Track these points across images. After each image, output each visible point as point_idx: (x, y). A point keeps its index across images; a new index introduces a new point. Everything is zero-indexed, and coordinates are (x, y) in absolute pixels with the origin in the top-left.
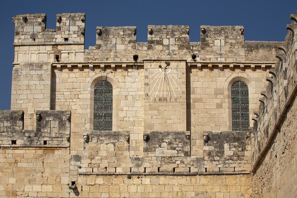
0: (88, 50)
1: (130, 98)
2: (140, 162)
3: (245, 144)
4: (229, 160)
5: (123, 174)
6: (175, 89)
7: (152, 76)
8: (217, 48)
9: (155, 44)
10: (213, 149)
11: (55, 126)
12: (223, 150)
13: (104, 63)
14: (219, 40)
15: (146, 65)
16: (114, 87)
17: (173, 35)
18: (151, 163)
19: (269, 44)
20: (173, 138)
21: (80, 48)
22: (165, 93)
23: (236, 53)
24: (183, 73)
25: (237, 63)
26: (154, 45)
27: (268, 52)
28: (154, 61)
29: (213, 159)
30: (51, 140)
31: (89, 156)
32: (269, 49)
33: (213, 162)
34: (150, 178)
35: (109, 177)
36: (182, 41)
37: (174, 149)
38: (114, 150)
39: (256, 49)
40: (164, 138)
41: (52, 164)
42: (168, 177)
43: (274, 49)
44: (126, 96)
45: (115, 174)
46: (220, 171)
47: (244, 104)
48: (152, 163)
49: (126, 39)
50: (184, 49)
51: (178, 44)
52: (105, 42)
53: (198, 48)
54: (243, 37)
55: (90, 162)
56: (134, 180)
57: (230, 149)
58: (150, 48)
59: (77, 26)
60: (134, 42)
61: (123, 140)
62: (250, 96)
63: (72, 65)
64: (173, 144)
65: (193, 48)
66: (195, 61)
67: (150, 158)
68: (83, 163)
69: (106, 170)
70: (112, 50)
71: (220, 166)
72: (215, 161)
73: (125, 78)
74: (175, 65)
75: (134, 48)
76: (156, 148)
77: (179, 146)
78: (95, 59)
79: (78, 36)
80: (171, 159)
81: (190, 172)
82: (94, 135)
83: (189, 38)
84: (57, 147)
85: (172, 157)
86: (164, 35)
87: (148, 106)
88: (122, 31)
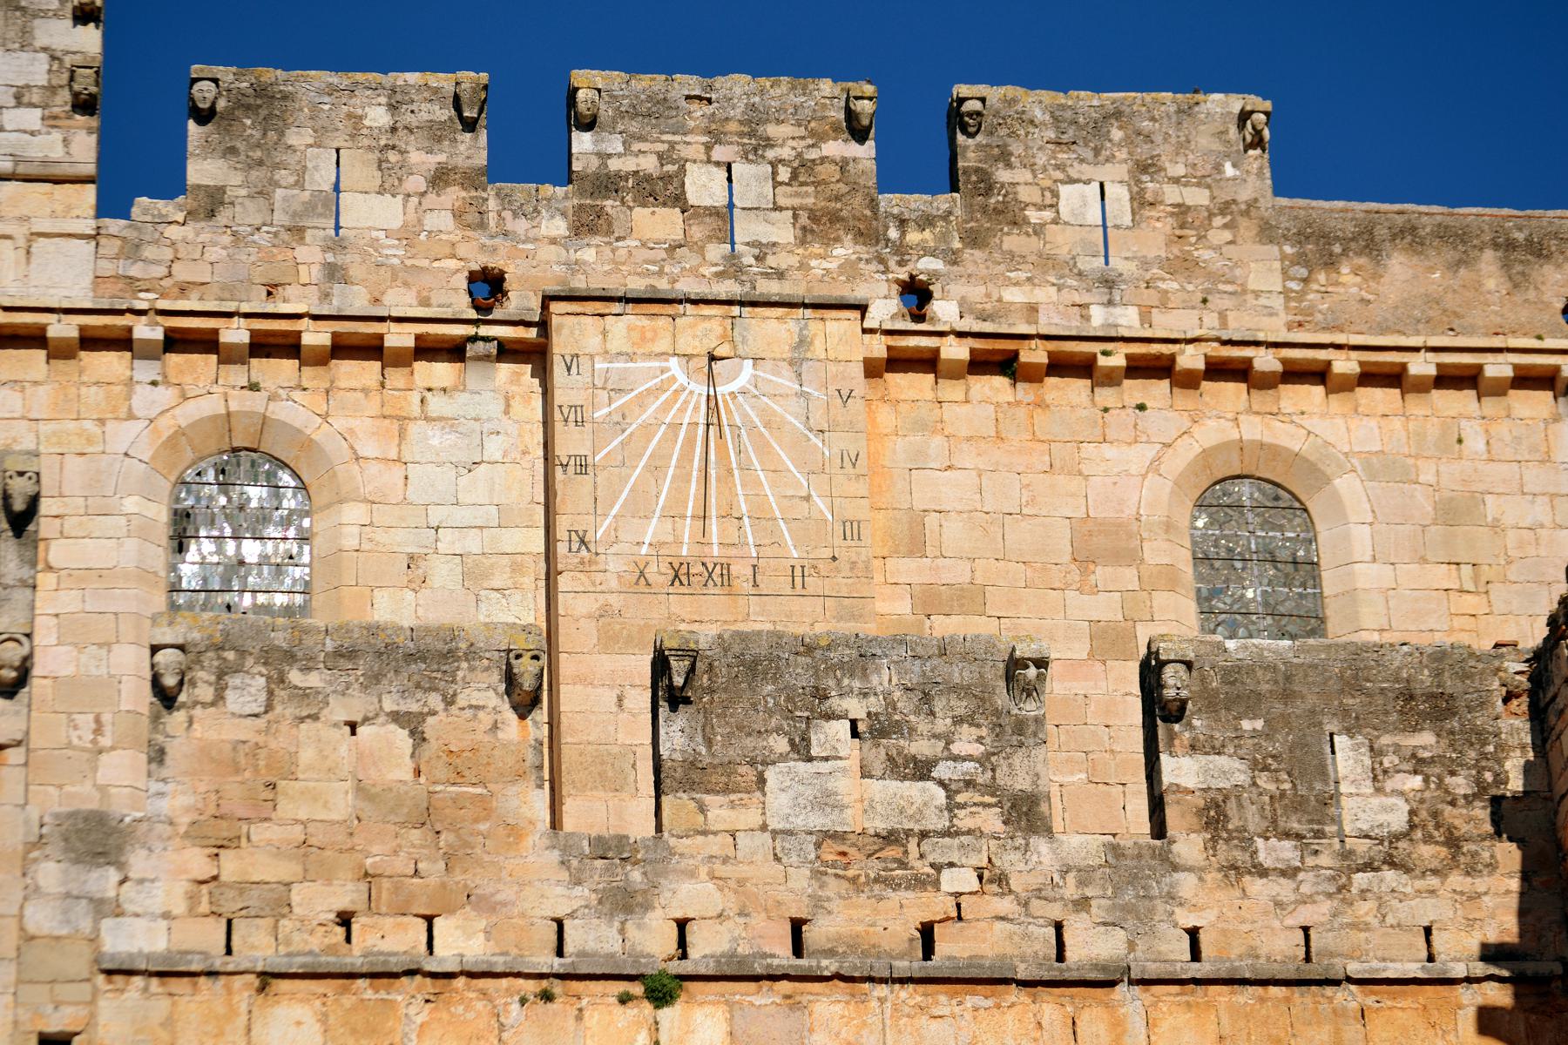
0: (123, 222)
2: (636, 875)
3: (1500, 747)
5: (499, 969)
6: (785, 502)
7: (613, 406)
9: (629, 198)
10: (1242, 778)
12: (1318, 786)
13: (247, 316)
14: (1087, 182)
15: (565, 331)
17: (757, 147)
18: (732, 884)
19: (1449, 221)
21: (69, 208)
23: (1215, 277)
24: (845, 393)
26: (623, 202)
29: (1241, 857)
31: (195, 817)
32: (1457, 256)
33: (1247, 878)
34: (727, 1002)
35: (369, 994)
36: (824, 182)
37: (921, 770)
38: (418, 773)
39: (1359, 254)
40: (832, 683)
42: (882, 1000)
43: (1489, 254)
44: (411, 557)
45: (428, 968)
46: (1308, 952)
47: (1293, 637)
48: (741, 882)
49: (415, 157)
50: (837, 240)
51: (796, 202)
52: (254, 174)
53: (944, 237)
54: (1261, 168)
55: (208, 871)
56: (593, 1018)
57: (1375, 778)
58: (587, 224)
59: (45, 49)
60: (471, 180)
62: (1330, 582)
64: (912, 730)
65: (903, 234)
67: (716, 845)
68: (141, 881)
69: (348, 939)
70: (309, 234)
71: (1305, 915)
72: (1263, 872)
73: (402, 434)
74: (785, 335)
75: (471, 219)
76: (765, 763)
77: (956, 748)
78: (183, 289)
79: (51, 121)
80: (892, 852)
81: (1061, 957)
82: (242, 653)
83: (871, 166)
85: (908, 833)
86: (688, 139)
88: (383, 100)
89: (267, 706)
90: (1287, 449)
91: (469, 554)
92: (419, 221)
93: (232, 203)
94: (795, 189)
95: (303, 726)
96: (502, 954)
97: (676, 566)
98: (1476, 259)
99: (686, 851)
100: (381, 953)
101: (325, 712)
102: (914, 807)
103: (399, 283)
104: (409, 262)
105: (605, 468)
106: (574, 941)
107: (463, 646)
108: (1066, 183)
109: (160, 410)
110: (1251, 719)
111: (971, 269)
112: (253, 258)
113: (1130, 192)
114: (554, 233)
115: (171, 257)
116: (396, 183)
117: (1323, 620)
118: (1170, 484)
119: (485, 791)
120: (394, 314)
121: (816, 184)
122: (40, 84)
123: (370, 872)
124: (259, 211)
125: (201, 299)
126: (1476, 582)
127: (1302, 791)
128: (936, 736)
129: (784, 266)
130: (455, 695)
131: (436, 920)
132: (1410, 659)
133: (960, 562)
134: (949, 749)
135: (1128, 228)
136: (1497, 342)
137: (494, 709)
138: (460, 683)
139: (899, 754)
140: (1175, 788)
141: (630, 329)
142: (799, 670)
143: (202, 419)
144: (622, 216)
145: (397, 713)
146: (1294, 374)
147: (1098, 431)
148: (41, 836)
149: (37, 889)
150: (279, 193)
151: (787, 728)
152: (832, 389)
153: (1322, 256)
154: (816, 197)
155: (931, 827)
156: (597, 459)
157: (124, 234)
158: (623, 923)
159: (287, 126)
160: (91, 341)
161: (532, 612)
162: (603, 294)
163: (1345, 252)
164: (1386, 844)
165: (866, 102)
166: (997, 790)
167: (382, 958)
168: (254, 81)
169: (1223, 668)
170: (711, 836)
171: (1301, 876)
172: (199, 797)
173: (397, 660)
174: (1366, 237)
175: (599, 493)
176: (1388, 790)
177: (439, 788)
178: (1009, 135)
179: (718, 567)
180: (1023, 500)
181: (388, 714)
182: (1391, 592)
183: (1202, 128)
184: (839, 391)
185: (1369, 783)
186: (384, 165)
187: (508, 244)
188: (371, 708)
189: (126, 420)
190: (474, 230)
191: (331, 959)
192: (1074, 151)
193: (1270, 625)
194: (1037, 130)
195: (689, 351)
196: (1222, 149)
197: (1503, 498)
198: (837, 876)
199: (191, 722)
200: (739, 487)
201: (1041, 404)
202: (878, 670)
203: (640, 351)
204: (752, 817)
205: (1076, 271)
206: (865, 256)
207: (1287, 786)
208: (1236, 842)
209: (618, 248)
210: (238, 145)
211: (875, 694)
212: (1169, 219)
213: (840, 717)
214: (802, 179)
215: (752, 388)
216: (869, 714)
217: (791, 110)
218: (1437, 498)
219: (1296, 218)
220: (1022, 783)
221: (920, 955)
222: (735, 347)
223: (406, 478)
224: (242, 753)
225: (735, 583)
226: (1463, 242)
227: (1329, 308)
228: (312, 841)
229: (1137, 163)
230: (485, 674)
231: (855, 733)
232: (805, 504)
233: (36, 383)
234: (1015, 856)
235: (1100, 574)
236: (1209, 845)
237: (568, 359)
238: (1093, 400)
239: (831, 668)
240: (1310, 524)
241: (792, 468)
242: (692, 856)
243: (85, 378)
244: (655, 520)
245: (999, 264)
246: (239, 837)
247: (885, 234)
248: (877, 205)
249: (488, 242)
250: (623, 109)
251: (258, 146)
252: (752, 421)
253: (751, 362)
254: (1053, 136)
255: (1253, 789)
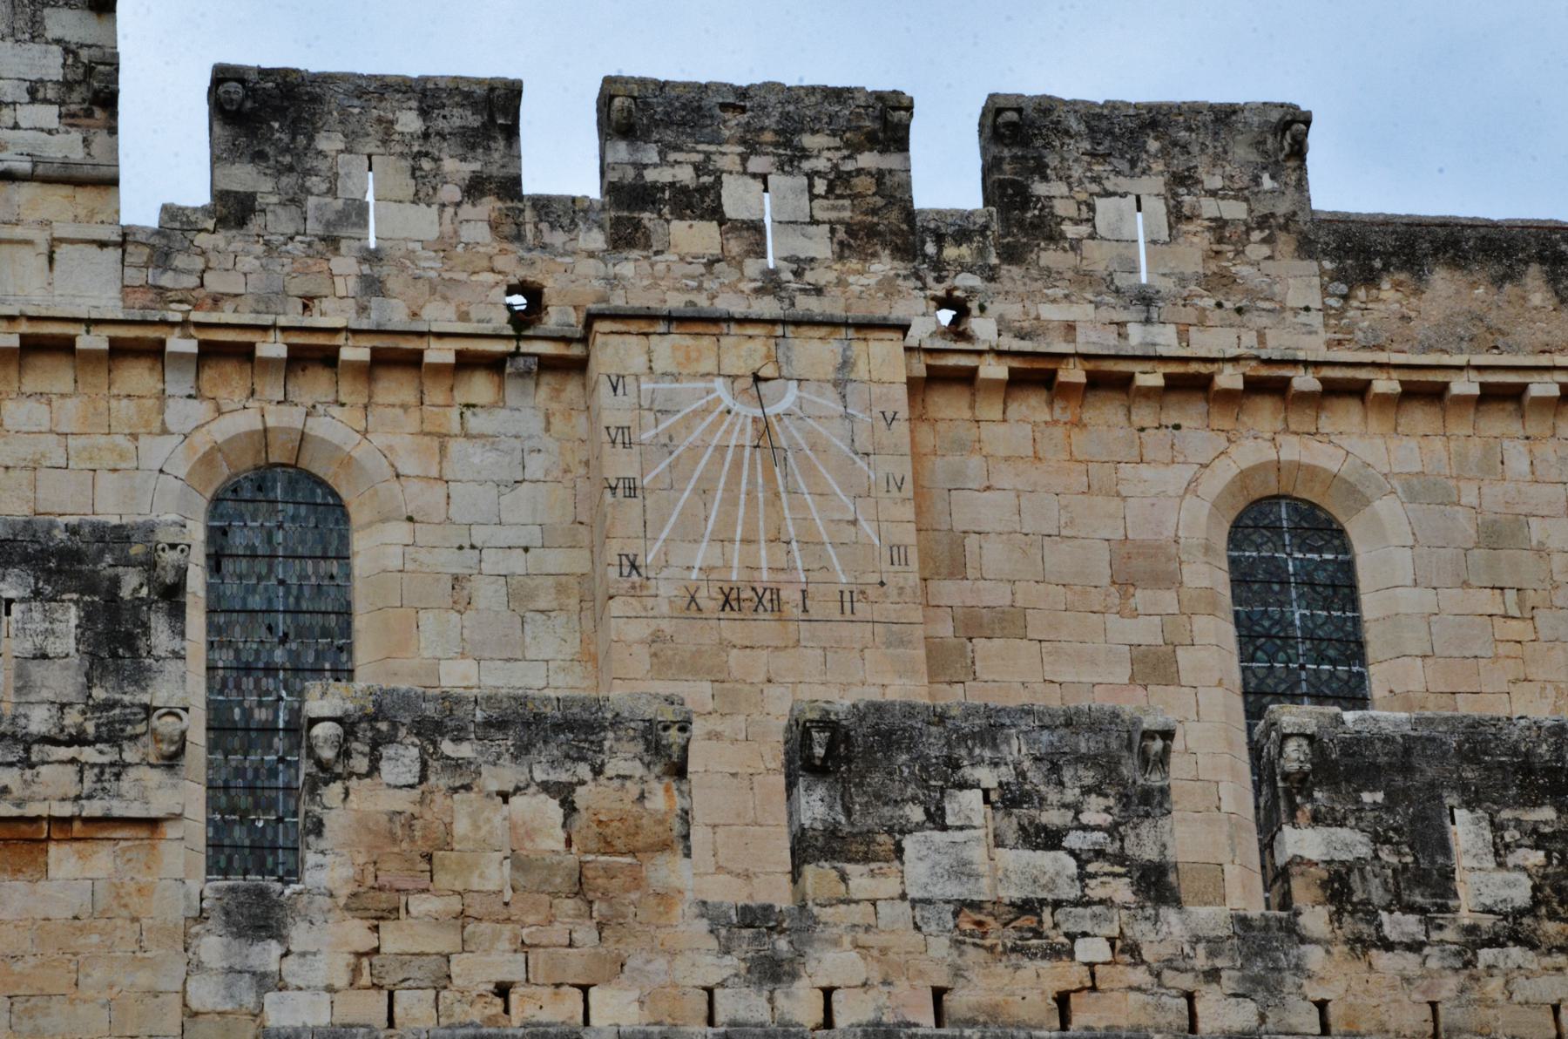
1: (488, 594)
2: (782, 944)
4: (1503, 945)
7: (661, 427)
8: (1119, 256)
9: (666, 210)
10: (1364, 851)
11: (53, 647)
12: (1440, 860)
13: (284, 329)
14: (1124, 195)
15: (610, 350)
16: (359, 514)
17: (792, 158)
18: (875, 953)
20: (1036, 759)
22: (763, 553)
24: (889, 415)
25: (1269, 362)
26: (660, 216)
27: (1494, 290)
28: (670, 318)
29: (1367, 930)
30: (10, 758)
32: (1499, 269)
33: (1373, 952)
37: (1051, 839)
38: (569, 842)
39: (1400, 269)
40: (963, 752)
41: (18, 967)
43: (1534, 269)
44: (456, 578)
46: (1436, 1027)
47: (1334, 662)
48: (884, 951)
49: (450, 165)
50: (874, 255)
51: (833, 215)
52: (285, 180)
53: (982, 252)
55: (369, 941)
57: (1497, 854)
58: (626, 237)
59: (58, 41)
61: (624, 759)
62: (1370, 605)
63: (23, 337)
64: (1042, 800)
65: (940, 249)
66: (964, 336)
67: (860, 913)
69: (507, 1011)
70: (344, 245)
72: (1388, 946)
73: (443, 449)
76: (902, 832)
77: (1086, 818)
78: (217, 300)
79: (68, 118)
80: (1027, 921)
84: (66, 821)
85: (1043, 902)
87: (642, 642)
88: (414, 104)
89: (420, 777)
90: (1325, 470)
91: (513, 575)
92: (456, 232)
93: (263, 211)
94: (832, 202)
95: (456, 796)
96: (656, 1024)
97: (727, 591)
98: (1522, 274)
99: (830, 920)
100: (539, 1024)
101: (480, 781)
102: (1047, 877)
103: (437, 297)
104: (447, 275)
105: (653, 491)
106: (725, 1010)
107: (609, 715)
108: (1102, 196)
109: (195, 425)
110: (1371, 791)
111: (1008, 285)
112: (287, 269)
113: (1167, 205)
114: (592, 246)
115: (202, 266)
116: (431, 192)
117: (1361, 645)
118: (1208, 505)
119: (634, 861)
120: (434, 329)
121: (854, 197)
122: (55, 79)
123: (527, 941)
124: (292, 220)
125: (235, 311)
126: (1521, 607)
127: (1424, 863)
128: (1065, 806)
129: (822, 282)
130: (603, 764)
131: (592, 991)
132: (1527, 733)
133: (1001, 584)
134: (1078, 820)
135: (1165, 243)
136: (1544, 360)
137: (641, 778)
138: (607, 752)
139: (1031, 823)
140: (1298, 860)
141: (674, 349)
142: (932, 740)
143: (238, 436)
144: (660, 230)
145: (547, 782)
146: (1335, 391)
147: (1135, 452)
148: (202, 910)
149: (200, 966)
150: (312, 201)
151: (922, 797)
152: (876, 411)
153: (1362, 271)
154: (853, 211)
155: (1064, 897)
156: (645, 482)
157: (152, 241)
158: (772, 992)
159: (317, 130)
160: (120, 351)
161: (578, 635)
162: (648, 312)
163: (1386, 268)
164: (1510, 919)
165: (903, 113)
166: (1126, 860)
167: (542, 1029)
168: (279, 80)
169: (1343, 741)
170: (853, 905)
171: (1427, 950)
172: (357, 869)
173: (545, 730)
174: (1407, 251)
175: (648, 517)
176: (1510, 865)
177: (590, 858)
178: (1044, 147)
179: (768, 592)
180: (1062, 522)
181: (538, 785)
182: (1434, 618)
183: (1239, 137)
184: (883, 413)
185: (1491, 857)
186: (418, 173)
187: (546, 256)
188: (523, 778)
189: (159, 435)
190: (511, 242)
191: (492, 1030)
192: (1110, 163)
193: (1309, 650)
194: (1072, 141)
195: (734, 372)
196: (1259, 160)
197: (1548, 520)
198: (975, 945)
199: (347, 793)
200: (786, 512)
201: (1078, 424)
202: (1007, 741)
203: (685, 372)
204: (890, 886)
205: (1113, 288)
206: (903, 272)
207: (1409, 859)
208: (1361, 915)
209: (657, 262)
210: (267, 149)
211: (1006, 764)
212: (1207, 234)
213: (972, 787)
214: (838, 192)
215: (797, 410)
216: (1000, 784)
217: (826, 119)
218: (1479, 521)
219: (1336, 231)
220: (1150, 854)
221: (1057, 1024)
222: (779, 369)
223: (448, 497)
224: (398, 824)
225: (785, 608)
226: (1509, 256)
227: (1370, 326)
228: (470, 912)
229: (1174, 175)
230: (632, 744)
231: (986, 800)
232: (852, 529)
233: (63, 396)
234: (1146, 926)
235: (1141, 597)
236: (1335, 917)
237: (614, 379)
238: (1129, 419)
239: (963, 739)
240: (1346, 548)
241: (838, 491)
242: (836, 925)
243: (114, 391)
244: (704, 544)
245: (1036, 280)
246: (397, 910)
247: (922, 249)
248: (914, 219)
249: (527, 255)
250: (657, 117)
251: (287, 150)
252: (797, 444)
253: (795, 383)
254: (1089, 147)
255: (1376, 862)
